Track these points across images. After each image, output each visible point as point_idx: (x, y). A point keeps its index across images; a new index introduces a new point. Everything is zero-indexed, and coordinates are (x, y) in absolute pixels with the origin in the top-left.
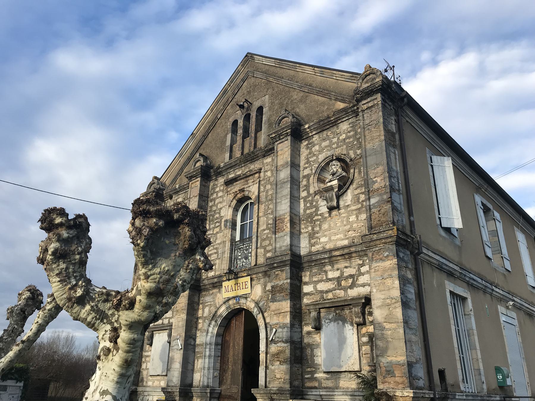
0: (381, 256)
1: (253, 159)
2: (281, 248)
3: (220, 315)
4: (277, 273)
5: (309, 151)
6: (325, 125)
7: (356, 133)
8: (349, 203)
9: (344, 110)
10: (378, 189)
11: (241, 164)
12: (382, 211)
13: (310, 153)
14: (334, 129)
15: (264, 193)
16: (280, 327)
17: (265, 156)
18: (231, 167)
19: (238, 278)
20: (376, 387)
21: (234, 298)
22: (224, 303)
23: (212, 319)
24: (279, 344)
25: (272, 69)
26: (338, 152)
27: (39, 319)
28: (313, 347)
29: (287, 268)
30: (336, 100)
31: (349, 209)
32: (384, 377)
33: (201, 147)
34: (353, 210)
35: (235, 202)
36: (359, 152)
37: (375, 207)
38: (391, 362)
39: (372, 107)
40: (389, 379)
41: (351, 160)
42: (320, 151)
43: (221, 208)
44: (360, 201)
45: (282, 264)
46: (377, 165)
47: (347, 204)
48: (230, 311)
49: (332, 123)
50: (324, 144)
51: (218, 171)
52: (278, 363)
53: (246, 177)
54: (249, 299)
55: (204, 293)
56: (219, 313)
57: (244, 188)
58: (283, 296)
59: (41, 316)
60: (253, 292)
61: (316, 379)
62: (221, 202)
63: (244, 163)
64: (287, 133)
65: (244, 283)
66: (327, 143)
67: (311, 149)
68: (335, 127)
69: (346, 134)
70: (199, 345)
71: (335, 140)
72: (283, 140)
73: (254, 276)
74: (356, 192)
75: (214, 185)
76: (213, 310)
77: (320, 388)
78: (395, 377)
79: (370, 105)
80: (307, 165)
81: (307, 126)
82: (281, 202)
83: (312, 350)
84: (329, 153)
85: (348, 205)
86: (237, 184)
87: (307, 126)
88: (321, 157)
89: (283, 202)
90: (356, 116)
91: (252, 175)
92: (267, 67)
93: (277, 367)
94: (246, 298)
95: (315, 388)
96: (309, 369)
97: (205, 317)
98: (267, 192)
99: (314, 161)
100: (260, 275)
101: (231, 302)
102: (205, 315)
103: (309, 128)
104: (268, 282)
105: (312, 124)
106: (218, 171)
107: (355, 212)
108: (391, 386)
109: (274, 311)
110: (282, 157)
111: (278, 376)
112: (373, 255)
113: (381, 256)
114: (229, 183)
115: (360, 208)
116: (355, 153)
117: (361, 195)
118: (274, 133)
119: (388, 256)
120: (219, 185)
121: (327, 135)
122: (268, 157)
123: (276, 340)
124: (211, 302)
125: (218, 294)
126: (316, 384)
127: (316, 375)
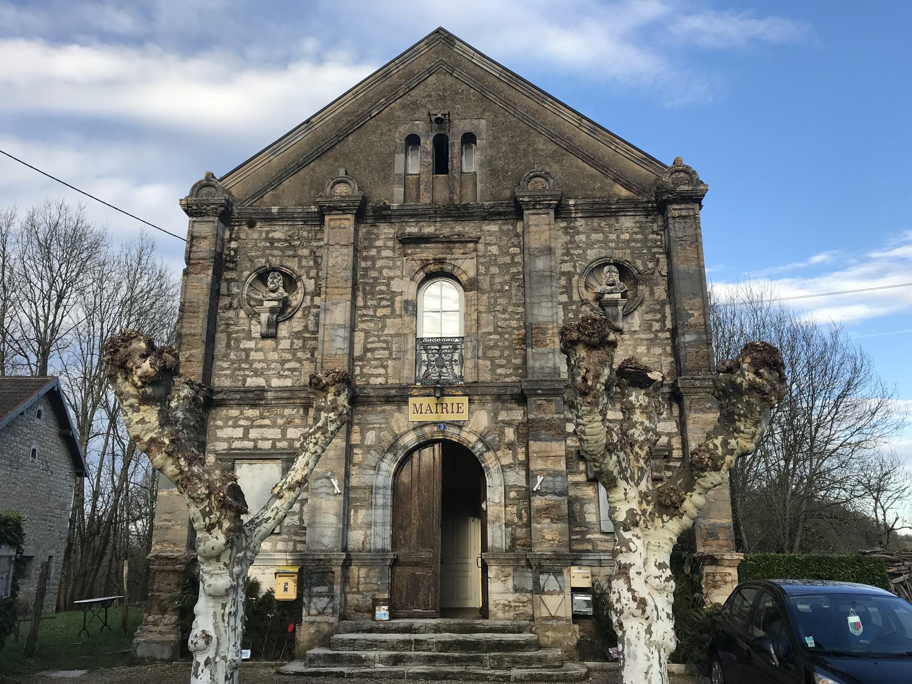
0: (702, 406)
1: (462, 217)
2: (542, 368)
3: (405, 447)
4: (539, 402)
5: (569, 238)
6: (599, 210)
7: (646, 240)
8: (636, 328)
9: (627, 200)
10: (695, 326)
11: (435, 217)
12: (701, 353)
13: (571, 242)
14: (612, 221)
15: (488, 278)
16: (549, 475)
17: (485, 219)
18: (413, 216)
19: (444, 395)
20: (694, 551)
21: (435, 423)
22: (414, 429)
24: (548, 497)
25: (491, 80)
26: (618, 255)
27: (316, 447)
28: (584, 501)
30: (616, 180)
31: (636, 336)
32: (705, 540)
33: (330, 154)
34: (642, 339)
35: (422, 275)
36: (651, 265)
37: (691, 346)
38: (714, 524)
39: (685, 217)
40: (710, 542)
41: (639, 273)
42: (590, 245)
43: (390, 278)
44: (654, 330)
46: (694, 294)
47: (633, 329)
49: (611, 212)
50: (594, 236)
51: (384, 213)
52: (549, 520)
53: (449, 242)
54: (466, 429)
55: (361, 408)
56: (402, 442)
57: (445, 259)
59: (320, 441)
60: (472, 419)
61: (589, 541)
62: (389, 268)
63: (441, 217)
64: (550, 205)
65: (455, 406)
66: (600, 236)
67: (573, 237)
68: (613, 219)
69: (631, 235)
70: (354, 488)
71: (613, 236)
72: (541, 211)
73: (476, 397)
74: (648, 317)
75: (368, 233)
76: (388, 437)
77: (594, 551)
78: (718, 539)
79: (684, 213)
80: (566, 258)
81: (572, 202)
82: (540, 303)
83: (582, 506)
84: (604, 253)
85: (635, 332)
86: (427, 248)
87: (572, 202)
88: (592, 254)
89: (543, 304)
90: (647, 216)
91: (461, 242)
92: (482, 73)
93: (546, 526)
94: (460, 427)
95: (588, 551)
96: (577, 529)
97: (369, 447)
98: (493, 276)
99: (579, 255)
101: (427, 429)
102: (368, 442)
103: (574, 205)
104: (502, 409)
105: (580, 202)
106: (384, 213)
107: (645, 343)
108: (714, 549)
109: (536, 453)
110: (537, 236)
111: (548, 537)
112: (691, 403)
113: (702, 406)
114: (407, 241)
115: (651, 339)
116: (645, 265)
117: (654, 323)
118: (529, 196)
119: (710, 408)
120: (382, 237)
121: (599, 225)
122: (493, 223)
123: (543, 491)
124: (380, 424)
125: (396, 414)
126: (590, 547)
127: (588, 537)
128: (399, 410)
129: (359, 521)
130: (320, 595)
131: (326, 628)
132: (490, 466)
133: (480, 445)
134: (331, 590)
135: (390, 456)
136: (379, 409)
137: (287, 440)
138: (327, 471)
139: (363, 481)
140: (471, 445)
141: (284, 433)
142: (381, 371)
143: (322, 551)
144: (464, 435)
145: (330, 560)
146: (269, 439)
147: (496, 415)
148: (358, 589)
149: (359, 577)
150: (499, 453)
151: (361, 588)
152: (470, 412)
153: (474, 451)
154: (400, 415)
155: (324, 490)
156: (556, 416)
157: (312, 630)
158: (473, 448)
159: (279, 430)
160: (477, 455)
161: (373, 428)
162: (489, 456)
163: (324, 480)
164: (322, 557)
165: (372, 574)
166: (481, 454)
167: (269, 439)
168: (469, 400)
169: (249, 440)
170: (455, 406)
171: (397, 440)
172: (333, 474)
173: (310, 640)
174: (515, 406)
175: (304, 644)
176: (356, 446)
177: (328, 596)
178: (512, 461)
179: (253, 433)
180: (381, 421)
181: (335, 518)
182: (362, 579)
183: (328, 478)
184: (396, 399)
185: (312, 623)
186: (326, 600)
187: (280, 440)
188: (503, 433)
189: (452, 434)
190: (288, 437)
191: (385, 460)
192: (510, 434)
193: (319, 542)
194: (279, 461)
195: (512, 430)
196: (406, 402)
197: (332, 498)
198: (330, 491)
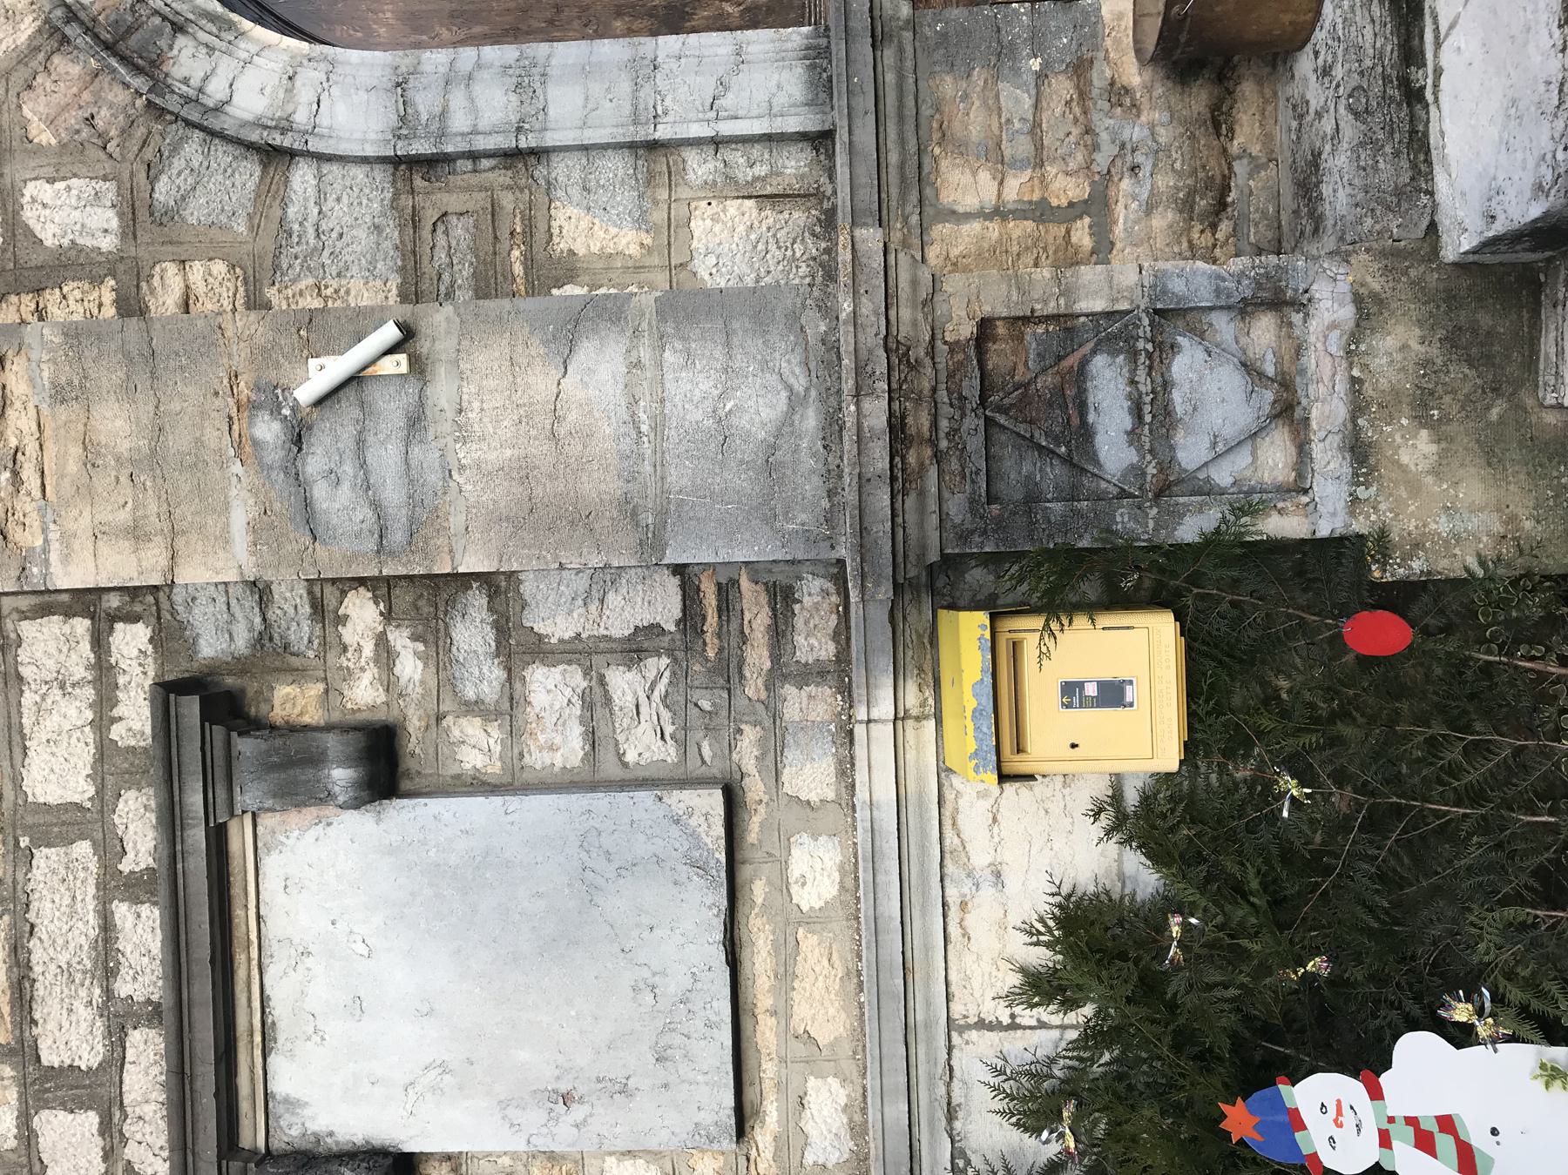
97: (136, 214)
129: (629, 241)
130: (1155, 416)
131: (1399, 345)
134: (1113, 331)
135: (186, 62)
137: (105, 800)
138: (246, 448)
139: (362, 238)
141: (61, 824)
143: (833, 425)
145: (893, 346)
146: (107, 926)
148: (1075, 210)
149: (999, 213)
151: (1067, 188)
155: (386, 457)
157: (1415, 450)
159: (47, 859)
163: (314, 463)
164: (876, 412)
167: (107, 926)
169: (116, 1061)
172: (271, 397)
173: (1491, 455)
175: (1522, 507)
177: (1164, 350)
179: (70, 1036)
181: (586, 352)
182: (1016, 187)
183: (298, 437)
185: (1360, 452)
186: (1186, 363)
187: (110, 849)
190: (80, 790)
191: (216, 90)
193: (770, 465)
194: (240, 838)
197: (442, 391)
198: (391, 408)
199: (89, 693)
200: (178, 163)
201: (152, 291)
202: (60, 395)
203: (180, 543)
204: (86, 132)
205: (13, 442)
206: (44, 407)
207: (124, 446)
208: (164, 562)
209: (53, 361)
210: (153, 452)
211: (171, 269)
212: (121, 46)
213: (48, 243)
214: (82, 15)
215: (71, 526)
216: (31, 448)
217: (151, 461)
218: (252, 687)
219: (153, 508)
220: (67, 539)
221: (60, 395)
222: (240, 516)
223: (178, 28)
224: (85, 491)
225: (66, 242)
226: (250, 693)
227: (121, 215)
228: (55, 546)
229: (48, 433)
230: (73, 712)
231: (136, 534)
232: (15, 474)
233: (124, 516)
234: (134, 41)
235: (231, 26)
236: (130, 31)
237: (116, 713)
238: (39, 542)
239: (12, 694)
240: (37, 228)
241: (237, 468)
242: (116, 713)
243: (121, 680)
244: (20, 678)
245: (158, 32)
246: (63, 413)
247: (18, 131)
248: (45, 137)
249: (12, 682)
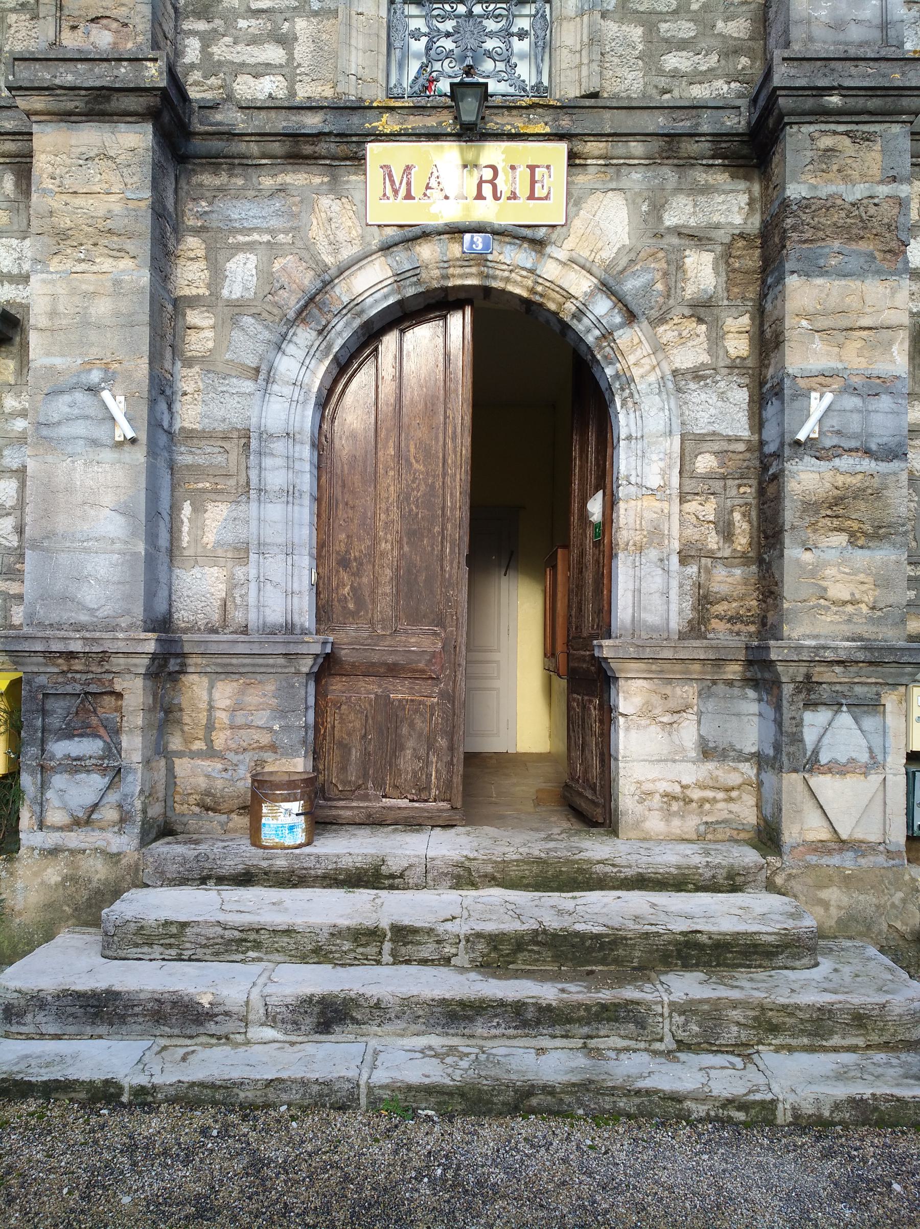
3: (353, 306)
4: (826, 142)
22: (386, 248)
23: (301, 316)
24: (845, 462)
29: (896, 129)
45: (874, 103)
48: (410, 292)
52: (843, 538)
55: (207, 179)
56: (342, 292)
58: (871, 257)
60: (577, 223)
70: (190, 435)
73: (593, 147)
93: (832, 555)
97: (238, 308)
100: (636, 148)
101: (427, 252)
102: (233, 290)
104: (678, 190)
109: (809, 317)
123: (828, 442)
125: (325, 201)
128: (335, 188)
129: (210, 538)
130: (75, 766)
131: (98, 871)
132: (636, 372)
133: (602, 307)
134: (113, 750)
135: (304, 336)
136: (267, 182)
138: (88, 365)
139: (219, 413)
140: (570, 307)
142: (273, 54)
143: (78, 627)
144: (550, 270)
145: (104, 656)
147: (657, 208)
148: (210, 742)
149: (211, 708)
150: (666, 333)
151: (220, 739)
152: (574, 200)
153: (579, 327)
154: (336, 206)
155: (80, 429)
156: (883, 190)
157: (53, 874)
158: (579, 314)
160: (590, 339)
161: (250, 247)
162: (625, 337)
163: (80, 396)
164: (76, 646)
165: (253, 698)
166: (607, 335)
168: (572, 156)
170: (523, 174)
171: (327, 284)
172: (110, 378)
173: (49, 906)
174: (721, 178)
175: (26, 918)
176: (193, 302)
177: (103, 771)
178: (705, 358)
180: (274, 223)
181: (120, 520)
182: (222, 717)
183: (93, 390)
184: (322, 148)
185: (54, 852)
186: (98, 781)
188: (680, 268)
189: (513, 270)
191: (290, 349)
192: (702, 271)
193: (65, 599)
195: (707, 258)
196: (358, 160)
197: (107, 455)
198: (100, 432)
199: (15, 271)
200: (260, 328)
201: (202, 312)
202: (117, 283)
203: (48, 333)
204: (278, 285)
205: (98, 260)
206: (110, 276)
207: (92, 310)
208: (40, 326)
209: (132, 281)
210: (89, 324)
211: (212, 322)
212: (312, 305)
213: (228, 265)
214: (328, 287)
215: (58, 284)
216: (95, 268)
217: (85, 323)
218: (15, 349)
219: (64, 322)
220: (53, 282)
221: (117, 283)
222: (58, 362)
223: (320, 332)
224: (73, 292)
225: (227, 273)
226: (11, 348)
227: (237, 300)
228: (50, 276)
229: (100, 276)
230: (6, 263)
231: (53, 314)
232: (84, 260)
233: (61, 308)
234: (316, 311)
235: (327, 355)
236: (320, 309)
237: (5, 283)
238: (52, 269)
239: (17, 234)
240: (234, 260)
241: (79, 361)
242: (5, 283)
243: (20, 287)
244: (24, 238)
245: (318, 323)
246: (109, 284)
247: (280, 253)
248: (277, 266)
249: (22, 235)
